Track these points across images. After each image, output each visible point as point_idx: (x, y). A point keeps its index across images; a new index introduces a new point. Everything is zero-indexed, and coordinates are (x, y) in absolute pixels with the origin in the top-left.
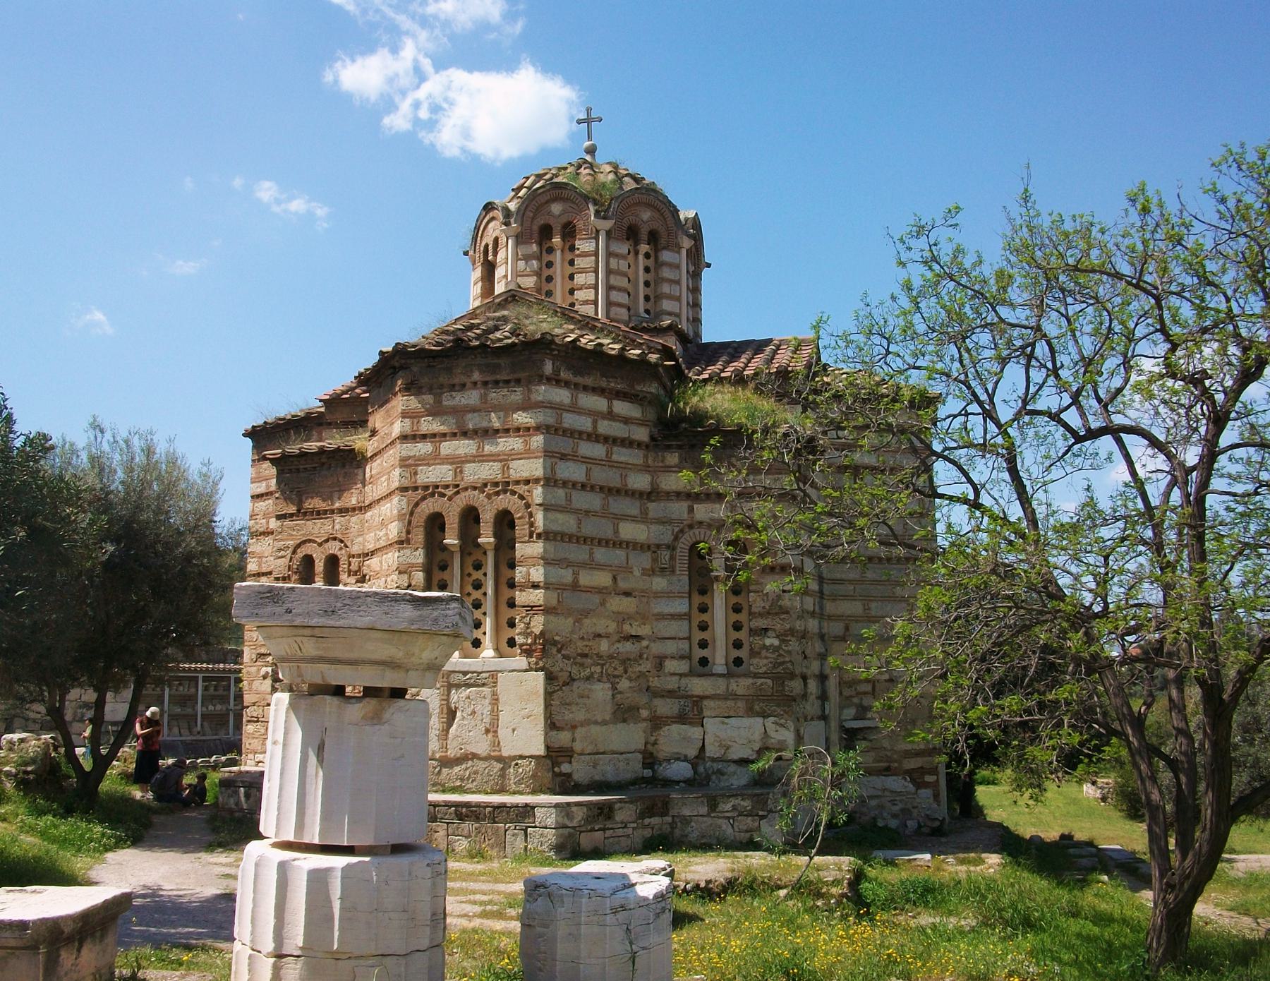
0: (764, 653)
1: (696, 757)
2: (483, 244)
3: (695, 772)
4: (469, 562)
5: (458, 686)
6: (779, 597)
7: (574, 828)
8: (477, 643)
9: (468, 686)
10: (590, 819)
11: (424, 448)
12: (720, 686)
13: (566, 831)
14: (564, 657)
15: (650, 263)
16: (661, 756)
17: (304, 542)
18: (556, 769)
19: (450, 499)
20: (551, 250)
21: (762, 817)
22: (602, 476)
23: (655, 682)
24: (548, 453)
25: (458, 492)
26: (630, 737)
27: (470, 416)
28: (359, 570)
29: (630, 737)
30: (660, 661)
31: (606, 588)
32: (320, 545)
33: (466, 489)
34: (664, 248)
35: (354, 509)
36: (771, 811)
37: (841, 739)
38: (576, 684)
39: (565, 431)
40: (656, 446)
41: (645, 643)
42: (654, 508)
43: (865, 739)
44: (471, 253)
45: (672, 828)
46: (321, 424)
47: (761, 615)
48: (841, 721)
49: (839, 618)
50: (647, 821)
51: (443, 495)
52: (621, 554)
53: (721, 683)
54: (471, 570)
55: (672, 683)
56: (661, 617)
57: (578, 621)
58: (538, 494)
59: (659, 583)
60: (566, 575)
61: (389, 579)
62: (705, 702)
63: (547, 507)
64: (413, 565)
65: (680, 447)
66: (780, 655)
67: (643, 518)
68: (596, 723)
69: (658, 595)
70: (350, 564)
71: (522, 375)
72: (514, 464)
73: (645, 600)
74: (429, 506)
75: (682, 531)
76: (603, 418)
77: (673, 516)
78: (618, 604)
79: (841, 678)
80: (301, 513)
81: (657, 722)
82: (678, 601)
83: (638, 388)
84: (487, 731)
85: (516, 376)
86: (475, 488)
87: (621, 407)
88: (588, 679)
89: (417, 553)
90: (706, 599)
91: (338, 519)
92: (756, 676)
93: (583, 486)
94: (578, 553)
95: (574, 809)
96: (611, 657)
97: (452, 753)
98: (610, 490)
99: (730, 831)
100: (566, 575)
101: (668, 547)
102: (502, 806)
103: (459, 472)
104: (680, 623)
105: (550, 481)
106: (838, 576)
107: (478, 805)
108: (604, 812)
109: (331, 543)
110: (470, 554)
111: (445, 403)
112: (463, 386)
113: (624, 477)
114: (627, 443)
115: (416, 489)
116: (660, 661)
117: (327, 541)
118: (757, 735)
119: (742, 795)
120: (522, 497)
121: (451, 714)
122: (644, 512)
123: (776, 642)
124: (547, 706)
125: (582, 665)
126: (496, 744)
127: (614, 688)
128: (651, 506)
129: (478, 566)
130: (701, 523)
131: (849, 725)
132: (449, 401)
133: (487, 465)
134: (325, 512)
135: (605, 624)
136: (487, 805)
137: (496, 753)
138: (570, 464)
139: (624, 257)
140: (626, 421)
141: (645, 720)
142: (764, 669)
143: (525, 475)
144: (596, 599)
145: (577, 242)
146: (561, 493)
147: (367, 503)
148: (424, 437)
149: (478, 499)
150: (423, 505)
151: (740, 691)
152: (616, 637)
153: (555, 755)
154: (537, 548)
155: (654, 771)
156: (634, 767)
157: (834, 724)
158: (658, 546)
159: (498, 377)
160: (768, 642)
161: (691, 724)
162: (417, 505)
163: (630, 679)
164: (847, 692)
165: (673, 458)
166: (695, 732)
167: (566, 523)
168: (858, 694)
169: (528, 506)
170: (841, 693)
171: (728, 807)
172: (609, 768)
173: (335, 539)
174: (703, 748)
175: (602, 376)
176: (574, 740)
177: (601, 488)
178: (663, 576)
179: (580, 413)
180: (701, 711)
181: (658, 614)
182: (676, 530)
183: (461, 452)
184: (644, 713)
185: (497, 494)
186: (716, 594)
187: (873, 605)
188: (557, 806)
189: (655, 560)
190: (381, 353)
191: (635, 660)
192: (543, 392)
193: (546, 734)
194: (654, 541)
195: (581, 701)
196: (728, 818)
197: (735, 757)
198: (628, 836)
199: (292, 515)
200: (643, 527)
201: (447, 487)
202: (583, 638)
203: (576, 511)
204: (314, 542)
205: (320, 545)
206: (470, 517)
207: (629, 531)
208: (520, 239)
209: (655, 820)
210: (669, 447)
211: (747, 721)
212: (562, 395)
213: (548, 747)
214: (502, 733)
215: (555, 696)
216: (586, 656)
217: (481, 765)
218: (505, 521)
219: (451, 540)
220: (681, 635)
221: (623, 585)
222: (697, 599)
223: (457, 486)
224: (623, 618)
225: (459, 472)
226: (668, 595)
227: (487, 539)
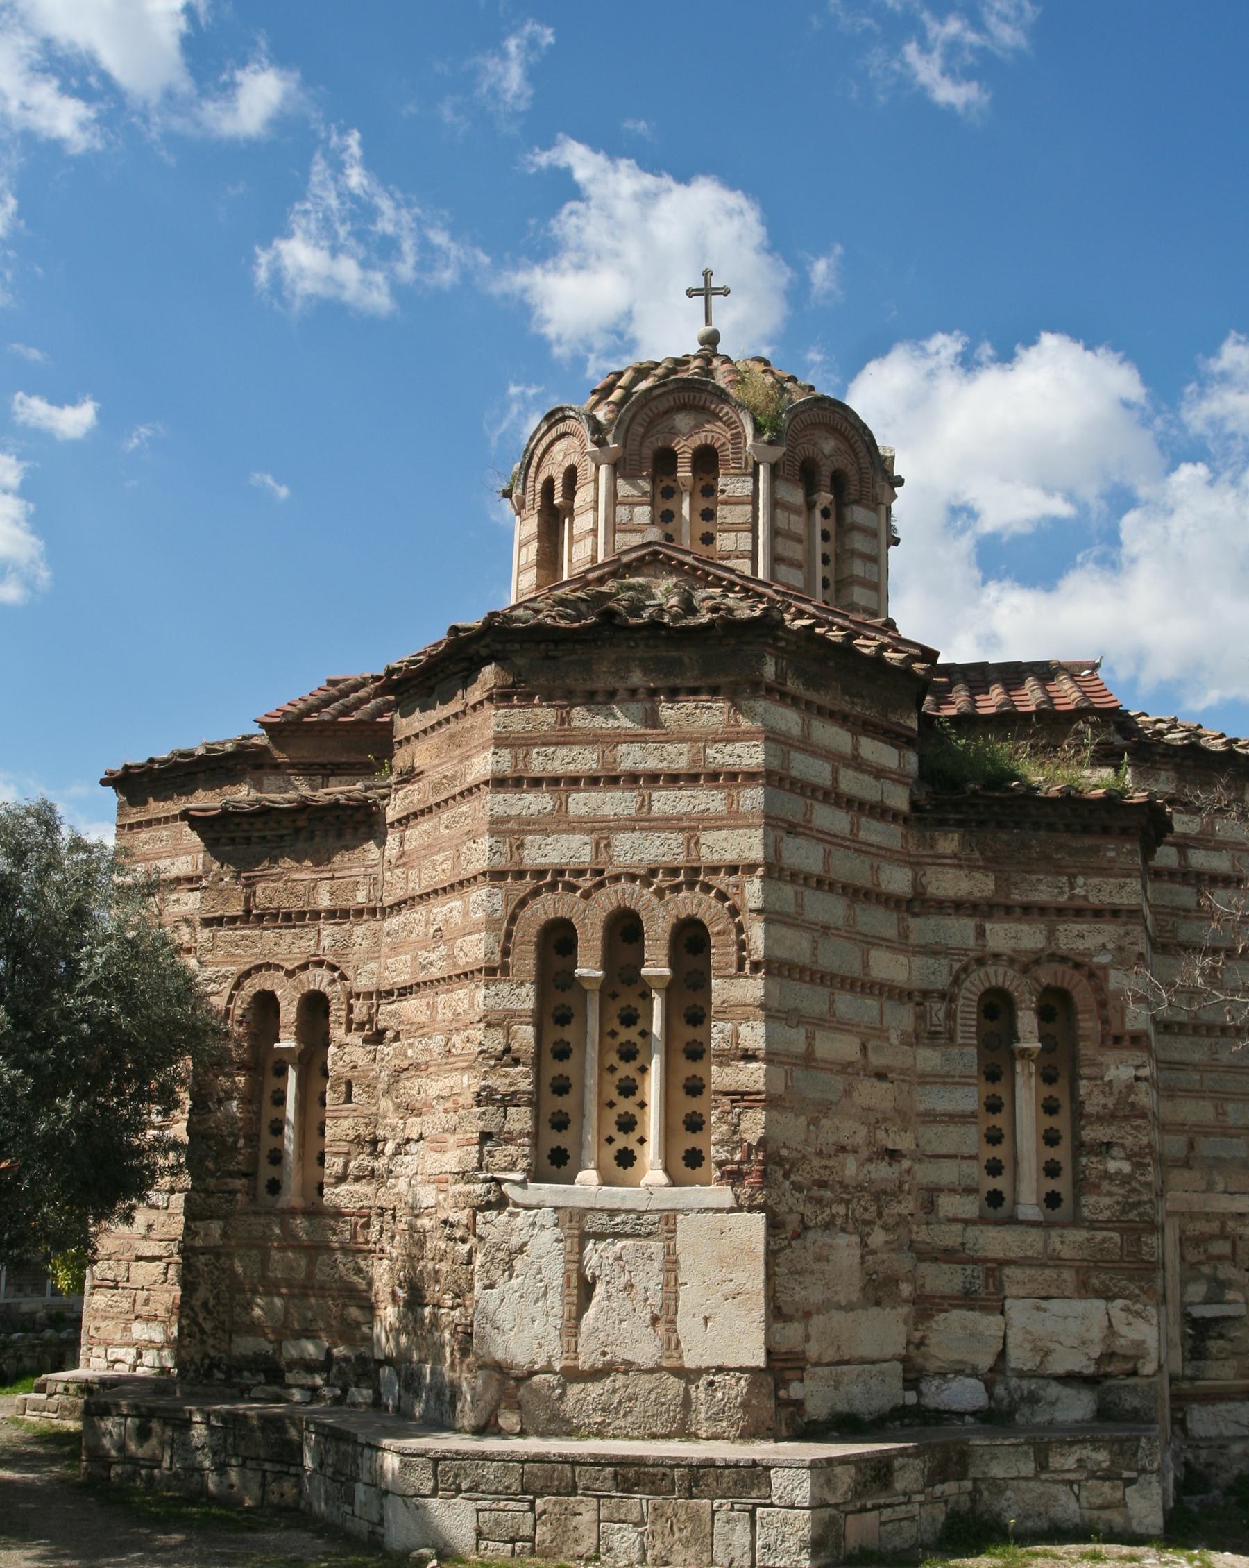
0: (1105, 1186)
1: (991, 1370)
2: (542, 477)
3: (991, 1396)
4: (615, 1008)
5: (600, 1237)
6: (1130, 1088)
7: (836, 1506)
8: (626, 1159)
9: (617, 1236)
10: (860, 1490)
11: (537, 802)
12: (1032, 1241)
13: (826, 1513)
14: (798, 1187)
15: (830, 525)
16: (932, 1365)
17: (258, 968)
18: (782, 1393)
19: (587, 895)
20: (669, 493)
21: (1130, 1482)
22: (849, 867)
23: (922, 1235)
24: (773, 822)
25: (601, 885)
26: (882, 1332)
27: (623, 748)
28: (371, 1020)
29: (882, 1332)
30: (930, 1196)
31: (850, 1064)
32: (290, 974)
33: (616, 878)
34: (857, 502)
35: (359, 912)
36: (1143, 1471)
37: (1184, 1336)
38: (811, 1235)
39: (794, 782)
40: (920, 820)
41: (906, 1164)
42: (923, 928)
43: (1221, 1336)
44: (518, 492)
45: (973, 1501)
46: (259, 767)
47: (1100, 1119)
48: (1184, 1305)
49: (1180, 1127)
50: (939, 1489)
51: (573, 888)
52: (871, 1004)
53: (1034, 1236)
54: (615, 1024)
55: (949, 1236)
56: (931, 1118)
57: (814, 1122)
58: (753, 892)
59: (929, 1058)
60: (796, 1039)
61: (456, 1039)
62: (1008, 1271)
63: (768, 915)
64: (512, 1014)
65: (960, 824)
66: (1133, 1190)
67: (901, 944)
68: (839, 1307)
69: (925, 1079)
70: (350, 1009)
71: (722, 680)
72: (709, 838)
73: (905, 1087)
74: (546, 907)
75: (965, 969)
76: (847, 766)
77: (952, 943)
78: (872, 1094)
79: (1182, 1231)
80: (251, 917)
81: (926, 1307)
82: (960, 1092)
83: (894, 718)
84: (655, 1320)
85: (712, 681)
86: (633, 878)
87: (876, 751)
88: (828, 1226)
89: (524, 991)
90: (1000, 1089)
91: (328, 929)
92: (1093, 1225)
93: (820, 882)
94: (812, 999)
95: (838, 1470)
96: (860, 1188)
97: (586, 1360)
98: (856, 891)
99: (1073, 1506)
100: (796, 1039)
101: (943, 996)
102: (709, 1464)
103: (603, 845)
104: (963, 1129)
105: (774, 871)
106: (1176, 1056)
107: (659, 1463)
108: (878, 1473)
109: (312, 972)
110: (614, 996)
111: (575, 723)
112: (611, 696)
113: (875, 870)
114: (880, 812)
115: (520, 875)
116: (930, 1196)
117: (305, 967)
118: (1096, 1333)
119: (1093, 1441)
120: (722, 896)
121: (586, 1289)
122: (904, 934)
123: (1126, 1168)
124: (770, 1276)
125: (819, 1201)
126: (673, 1345)
127: (864, 1245)
128: (914, 923)
129: (629, 1019)
130: (996, 956)
131: (1200, 1311)
133: (656, 838)
134: (302, 915)
135: (851, 1131)
136: (677, 1463)
137: (673, 1363)
138: (800, 841)
139: (798, 513)
140: (879, 773)
141: (906, 1301)
142: (1107, 1213)
143: (731, 856)
144: (839, 1082)
145: (722, 481)
146: (788, 891)
147: (388, 901)
148: (536, 782)
149: (640, 898)
150: (535, 905)
151: (1067, 1253)
152: (865, 1153)
153: (781, 1365)
154: (753, 988)
155: (920, 1394)
156: (888, 1392)
157: (1173, 1310)
158: (926, 994)
159: (679, 682)
160: (1112, 1166)
161: (983, 1309)
162: (523, 903)
163: (885, 1228)
164: (1193, 1255)
165: (949, 843)
166: (990, 1324)
167: (798, 946)
168: (1210, 1258)
169: (734, 911)
170: (1183, 1258)
171: (1070, 1462)
172: (857, 1390)
173: (320, 964)
174: (1002, 1355)
175: (846, 691)
176: (807, 1338)
177: (844, 887)
178: (934, 1046)
179: (814, 754)
180: (1000, 1287)
181: (926, 1114)
182: (957, 966)
183: (608, 811)
184: (906, 1289)
185: (676, 889)
186: (1019, 1081)
187: (1230, 1107)
188: (814, 1466)
189: (920, 1017)
190: (454, 630)
191: (893, 1194)
193: (768, 1329)
194: (918, 983)
195: (816, 1266)
196: (1070, 1483)
197: (1060, 1369)
198: (912, 1519)
199: (233, 920)
200: (902, 959)
201: (580, 873)
202: (820, 1154)
203: (807, 926)
204: (278, 967)
205: (290, 974)
206: (625, 929)
207: (889, 966)
208: (620, 468)
209: (950, 1488)
210: (942, 823)
211: (1079, 1306)
213: (769, 1353)
214: (680, 1324)
215: (781, 1258)
216: (822, 1184)
217: (644, 1383)
218: (690, 940)
219: (588, 968)
220: (966, 1151)
221: (876, 1060)
222: (989, 1089)
223: (600, 872)
224: (877, 1121)
225: (603, 845)
226: (944, 1080)
227: (656, 967)
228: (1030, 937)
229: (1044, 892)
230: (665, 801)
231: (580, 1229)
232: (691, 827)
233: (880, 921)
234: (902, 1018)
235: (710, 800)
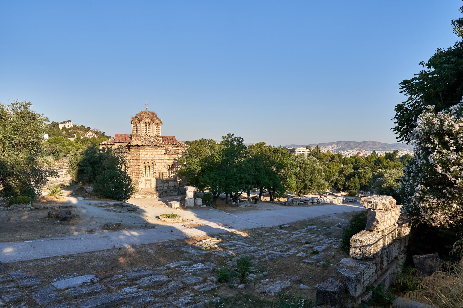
11: (143, 156)
22: (161, 158)
26: (162, 185)
29: (162, 185)
42: (164, 161)
59: (165, 169)
81: (164, 183)
87: (163, 151)
94: (159, 167)
132: (146, 150)
165: (166, 156)
207: (163, 164)
212: (157, 151)
230: (151, 156)
232: (152, 157)
233: (162, 161)
234: (163, 167)
235: (153, 156)
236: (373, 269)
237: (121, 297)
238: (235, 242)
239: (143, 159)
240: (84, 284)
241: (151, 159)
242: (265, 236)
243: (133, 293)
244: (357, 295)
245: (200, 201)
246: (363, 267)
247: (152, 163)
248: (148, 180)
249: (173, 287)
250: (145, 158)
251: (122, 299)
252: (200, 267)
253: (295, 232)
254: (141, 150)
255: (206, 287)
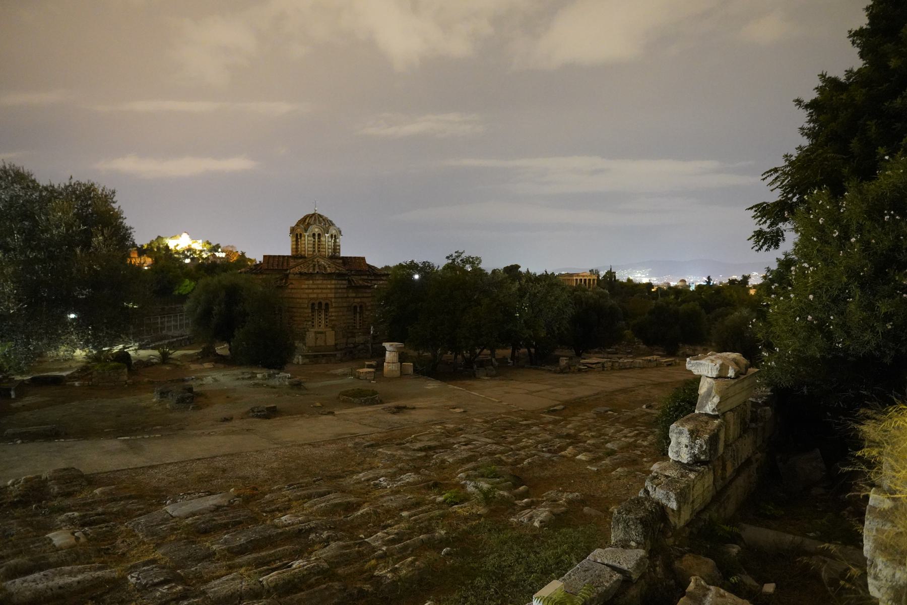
74: (312, 302)
81: (348, 338)
87: (344, 282)
153: (336, 345)
192: (333, 282)
207: (345, 304)
227: (323, 307)
228: (359, 300)
229: (360, 295)
230: (324, 291)
231: (316, 333)
232: (327, 293)
236: (709, 479)
237: (280, 531)
238: (470, 437)
239: (312, 296)
240: (218, 508)
241: (325, 296)
242: (522, 425)
243: (301, 522)
244: (682, 523)
245: (409, 366)
246: (692, 476)
247: (327, 304)
248: (321, 333)
249: (367, 514)
250: (315, 296)
251: (281, 533)
252: (411, 480)
253: (574, 418)
254: (307, 282)
255: (422, 512)
